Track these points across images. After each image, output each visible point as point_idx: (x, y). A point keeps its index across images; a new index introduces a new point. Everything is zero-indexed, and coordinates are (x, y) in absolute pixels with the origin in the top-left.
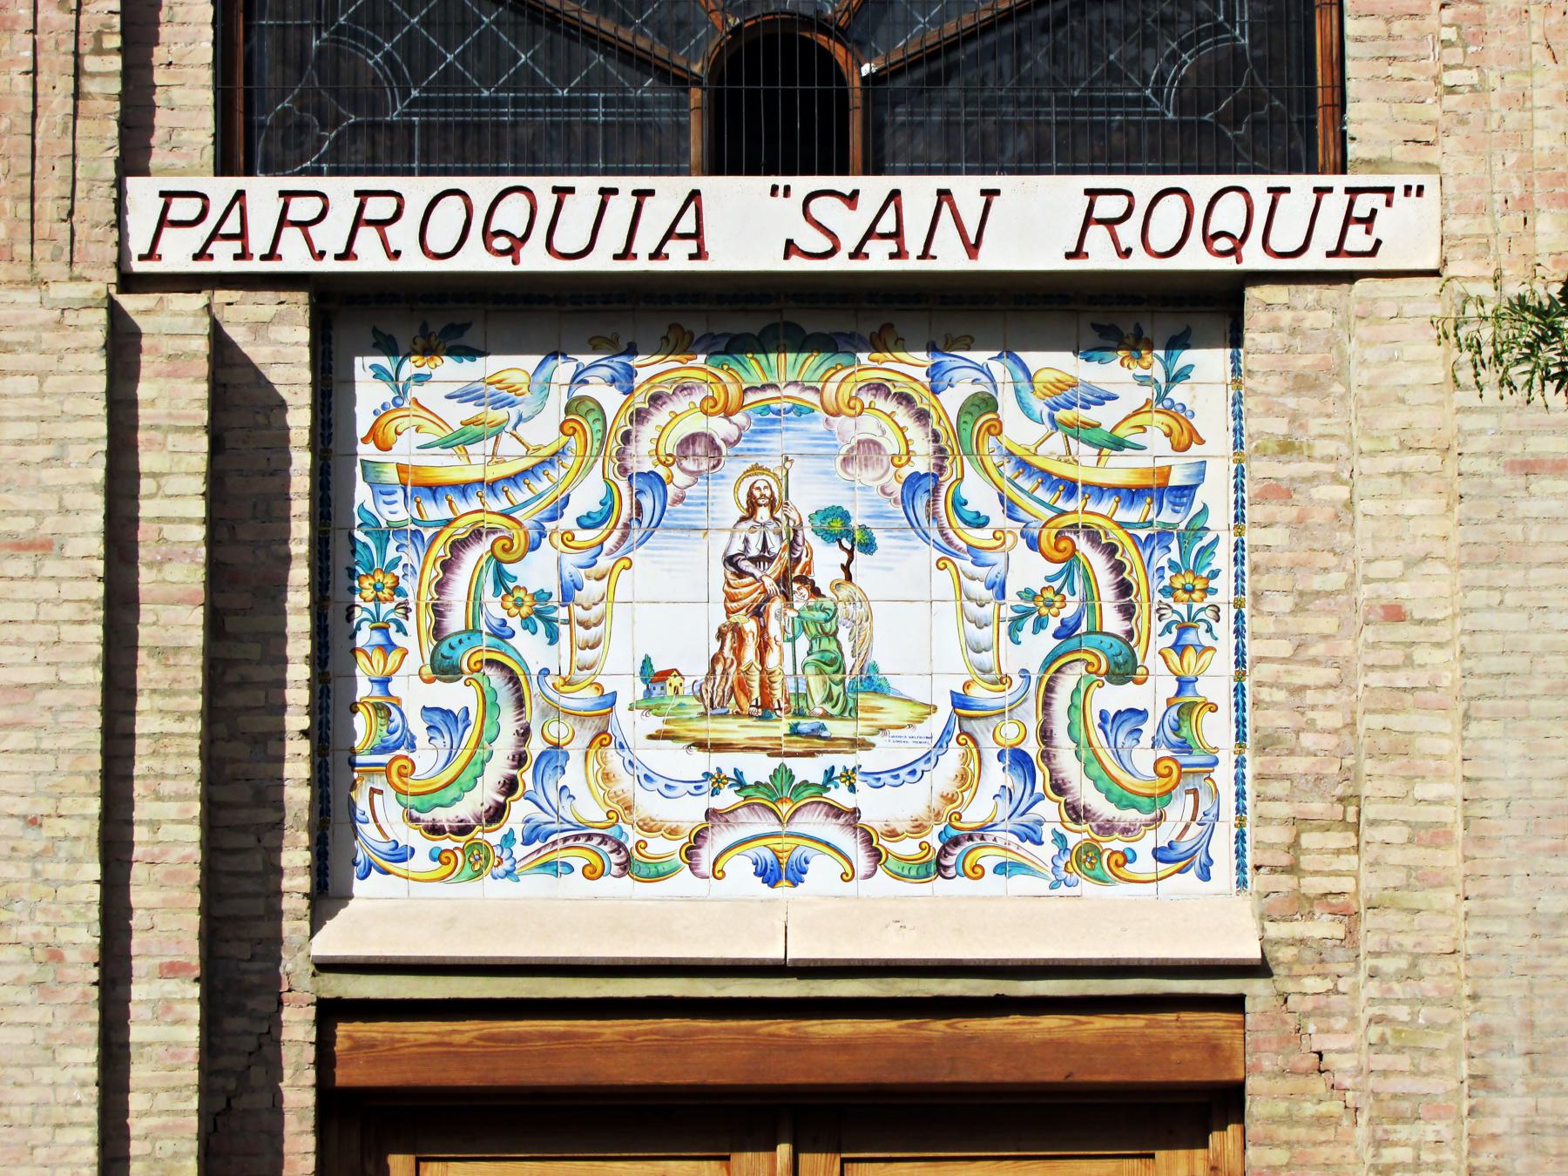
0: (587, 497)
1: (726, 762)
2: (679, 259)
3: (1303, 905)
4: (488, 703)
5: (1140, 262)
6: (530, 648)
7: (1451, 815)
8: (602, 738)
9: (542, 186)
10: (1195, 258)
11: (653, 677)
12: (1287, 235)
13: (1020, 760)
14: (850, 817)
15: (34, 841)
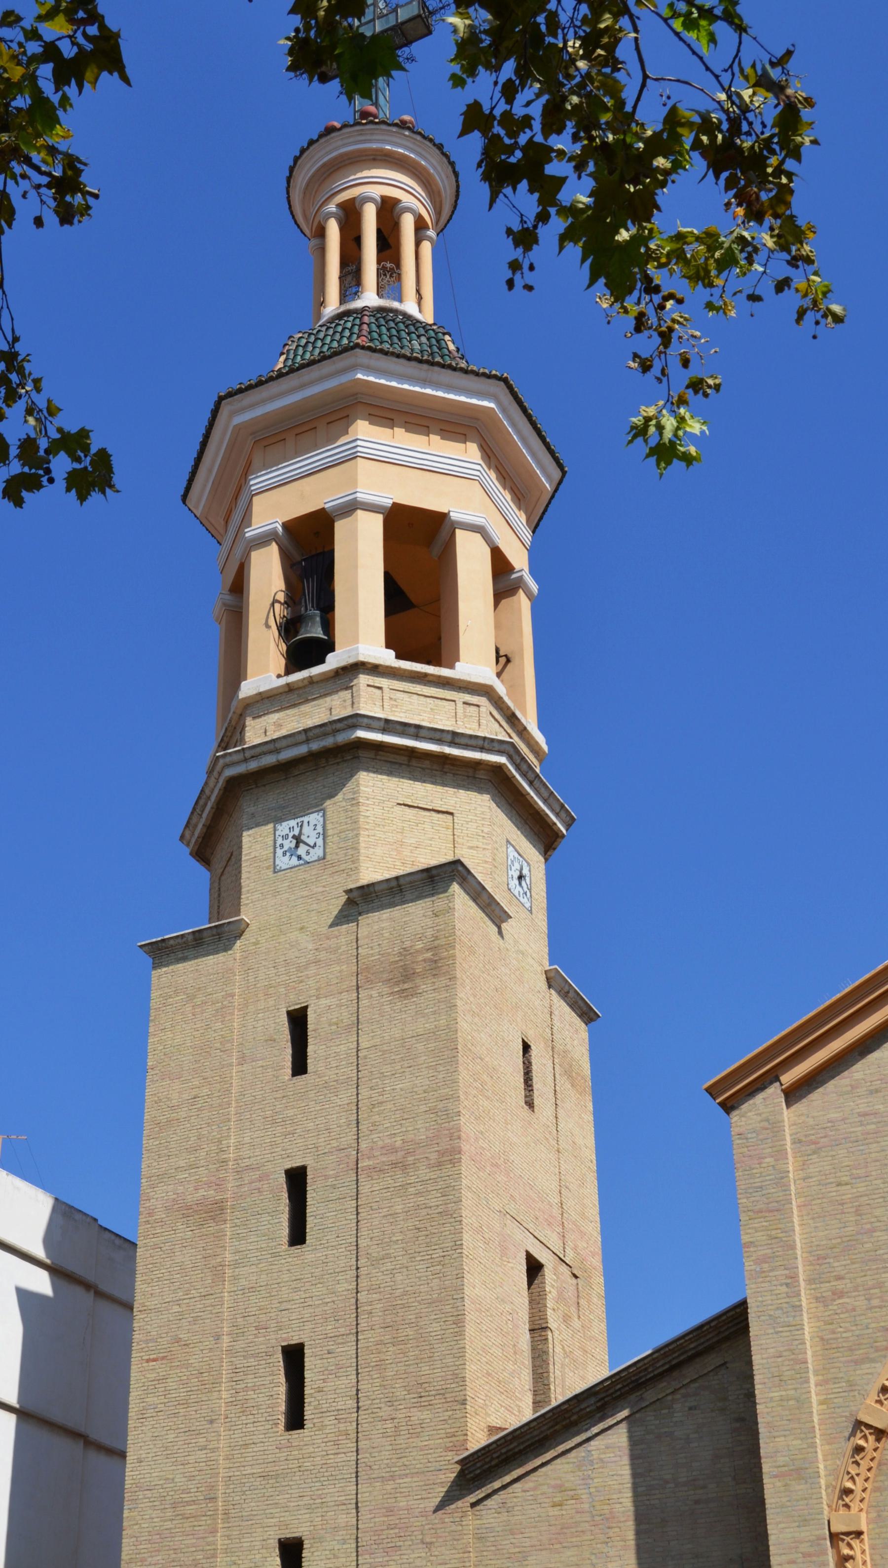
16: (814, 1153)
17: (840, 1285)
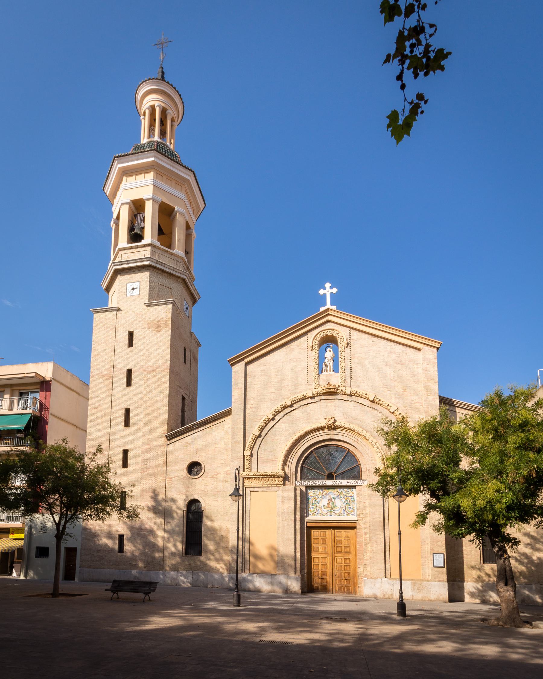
0: (320, 497)
1: (328, 510)
2: (325, 485)
3: (360, 517)
4: (315, 507)
5: (350, 484)
6: (317, 504)
7: (368, 513)
8: (321, 509)
9: (318, 481)
10: (353, 484)
11: (324, 506)
12: (359, 483)
13: (344, 510)
14: (335, 513)
15: (291, 514)
16: (250, 377)
17: (252, 406)
